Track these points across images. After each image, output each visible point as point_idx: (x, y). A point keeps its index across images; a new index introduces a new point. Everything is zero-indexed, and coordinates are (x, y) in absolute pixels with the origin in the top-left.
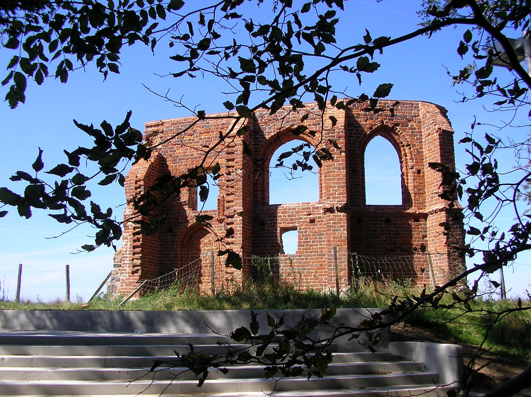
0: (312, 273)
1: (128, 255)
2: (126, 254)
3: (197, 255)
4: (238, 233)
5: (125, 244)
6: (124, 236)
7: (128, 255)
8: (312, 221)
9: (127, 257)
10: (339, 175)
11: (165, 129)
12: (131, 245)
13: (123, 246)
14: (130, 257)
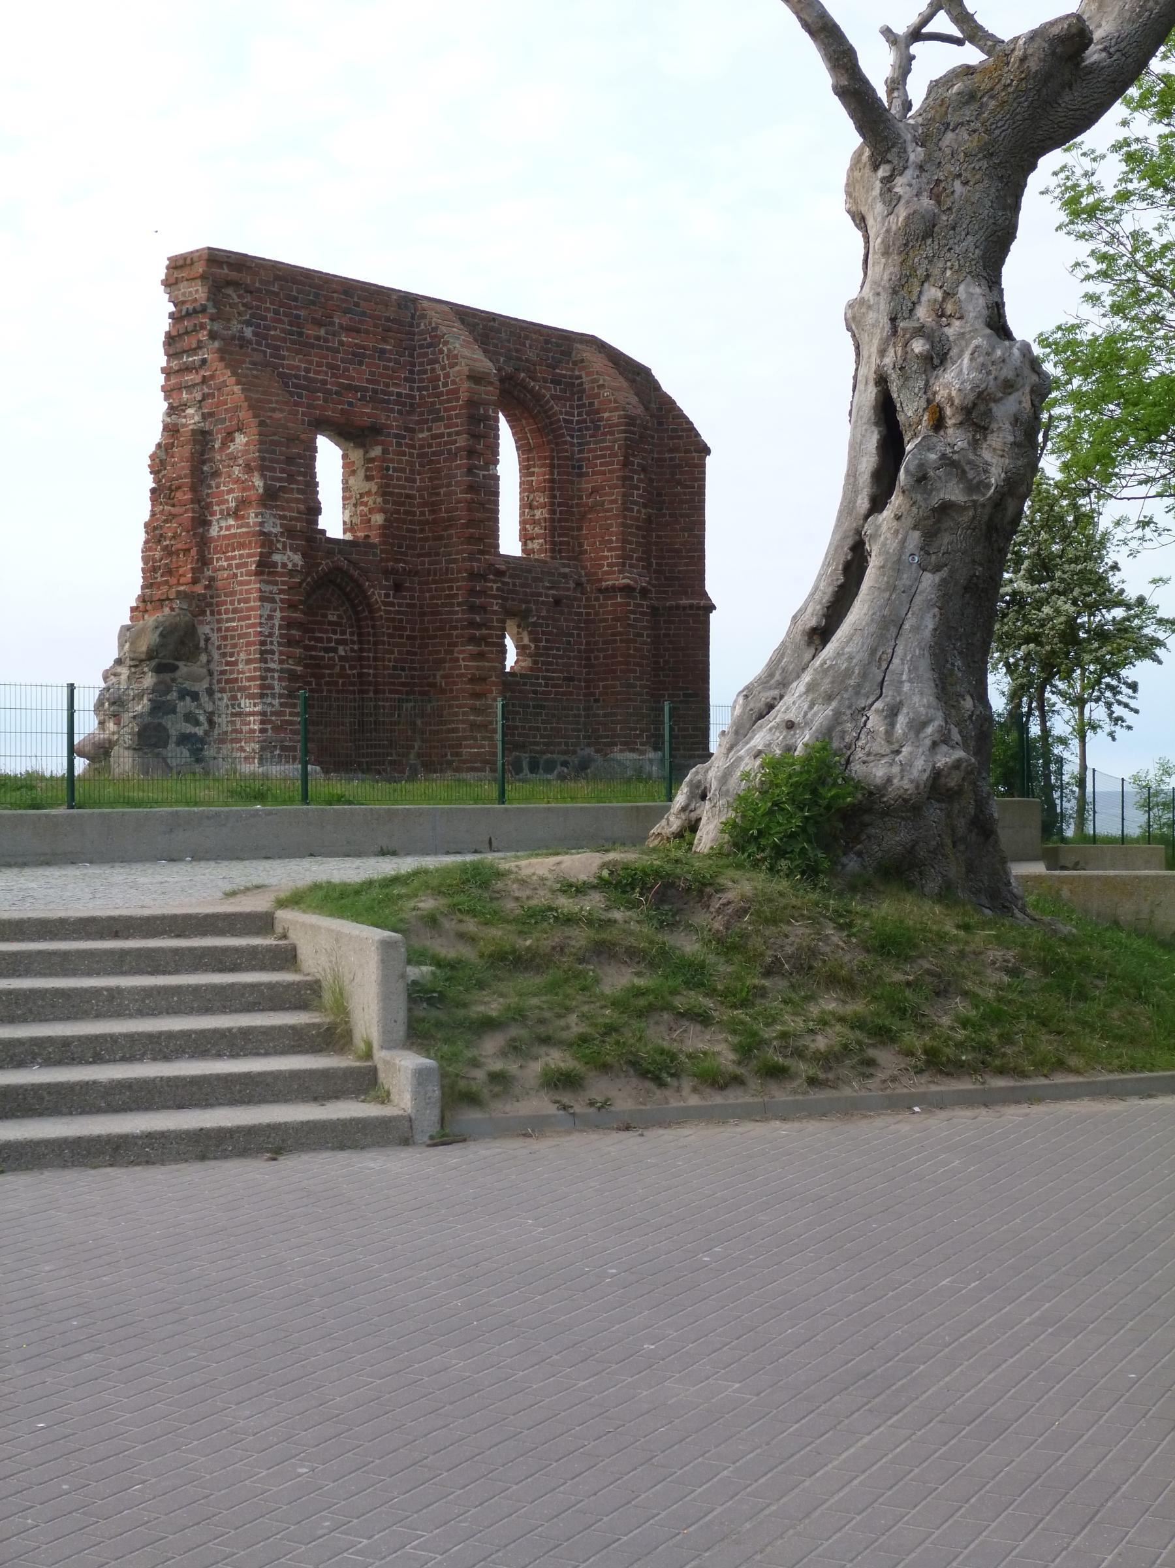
0: (554, 716)
1: (275, 648)
2: (272, 643)
3: (313, 653)
4: (495, 617)
5: (268, 615)
6: (265, 592)
7: (275, 648)
8: (557, 602)
9: (272, 652)
10: (637, 519)
11: (257, 285)
12: (282, 619)
13: (263, 621)
14: (281, 653)
